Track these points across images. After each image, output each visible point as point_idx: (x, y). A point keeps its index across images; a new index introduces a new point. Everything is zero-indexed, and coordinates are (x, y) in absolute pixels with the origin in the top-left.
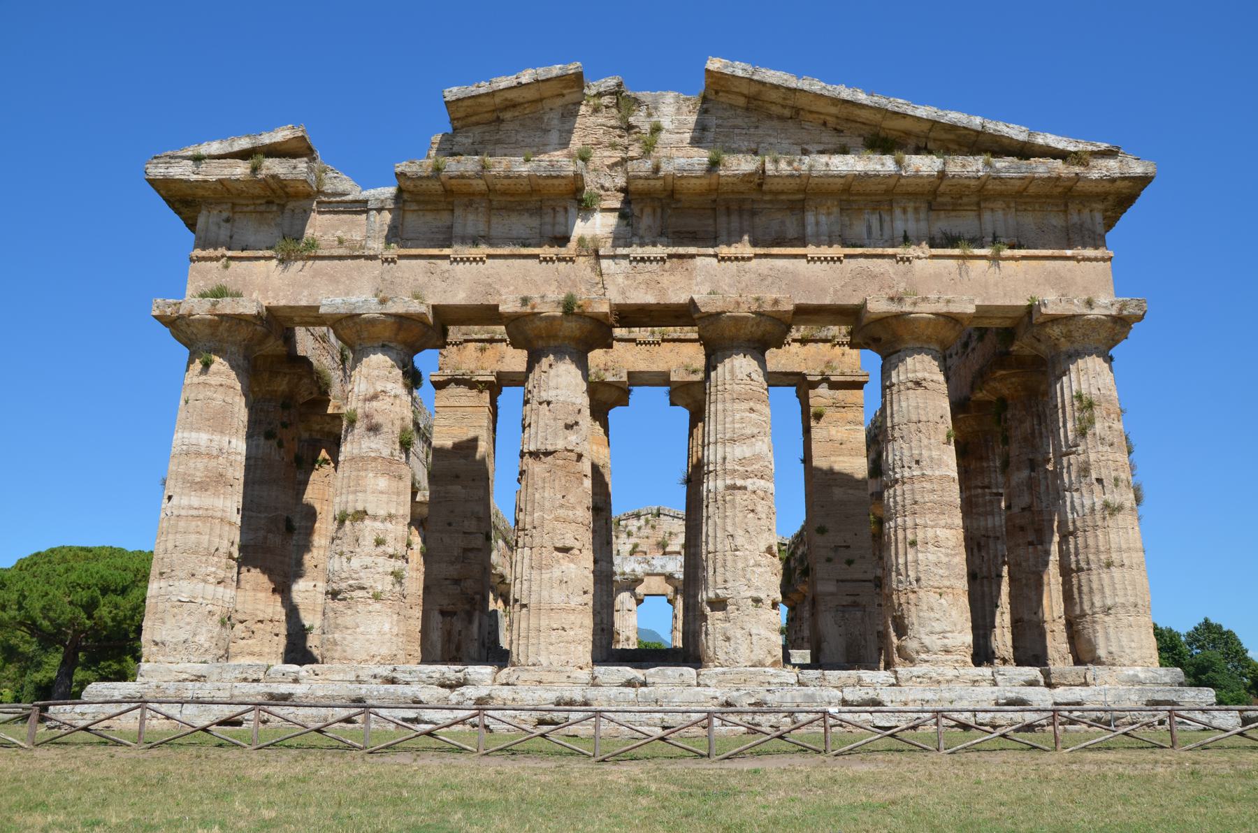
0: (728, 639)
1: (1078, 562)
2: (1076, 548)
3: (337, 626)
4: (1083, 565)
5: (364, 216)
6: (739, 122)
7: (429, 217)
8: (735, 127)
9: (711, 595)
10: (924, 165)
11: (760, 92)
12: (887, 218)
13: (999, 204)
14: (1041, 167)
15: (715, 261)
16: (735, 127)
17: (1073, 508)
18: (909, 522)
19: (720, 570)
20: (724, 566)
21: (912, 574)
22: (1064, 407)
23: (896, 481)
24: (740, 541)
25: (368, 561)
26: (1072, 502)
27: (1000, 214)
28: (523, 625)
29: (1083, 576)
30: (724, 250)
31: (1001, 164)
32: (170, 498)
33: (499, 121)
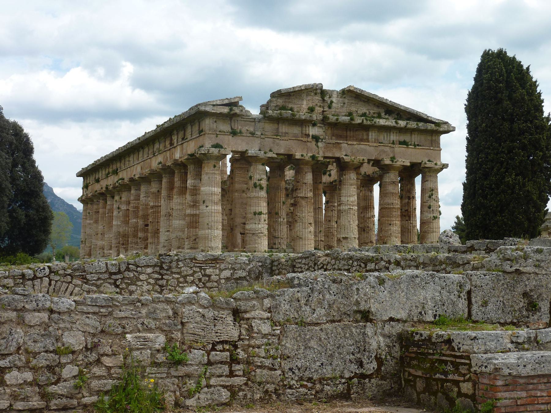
3: (256, 243)
5: (253, 123)
6: (353, 101)
7: (271, 125)
8: (352, 103)
12: (389, 134)
13: (416, 133)
14: (431, 126)
15: (346, 145)
16: (352, 103)
21: (390, 233)
24: (352, 223)
25: (263, 226)
27: (416, 136)
30: (349, 143)
31: (421, 124)
32: (207, 206)
33: (290, 95)
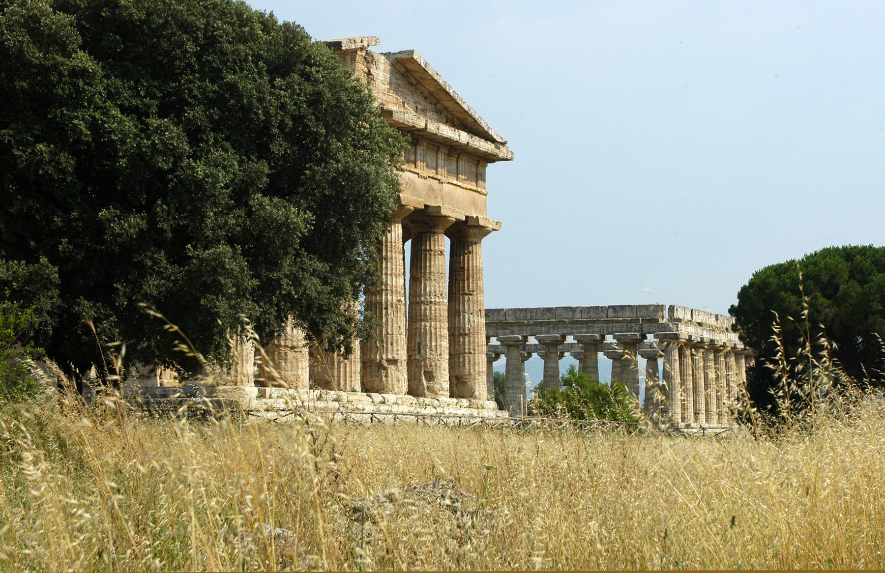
0: (398, 381)
1: (469, 349)
2: (469, 342)
4: (472, 351)
9: (390, 357)
10: (463, 137)
11: (415, 71)
17: (469, 321)
18: (438, 326)
19: (395, 344)
20: (397, 343)
22: (468, 270)
23: (431, 302)
26: (469, 319)
28: (348, 369)
29: (471, 356)
